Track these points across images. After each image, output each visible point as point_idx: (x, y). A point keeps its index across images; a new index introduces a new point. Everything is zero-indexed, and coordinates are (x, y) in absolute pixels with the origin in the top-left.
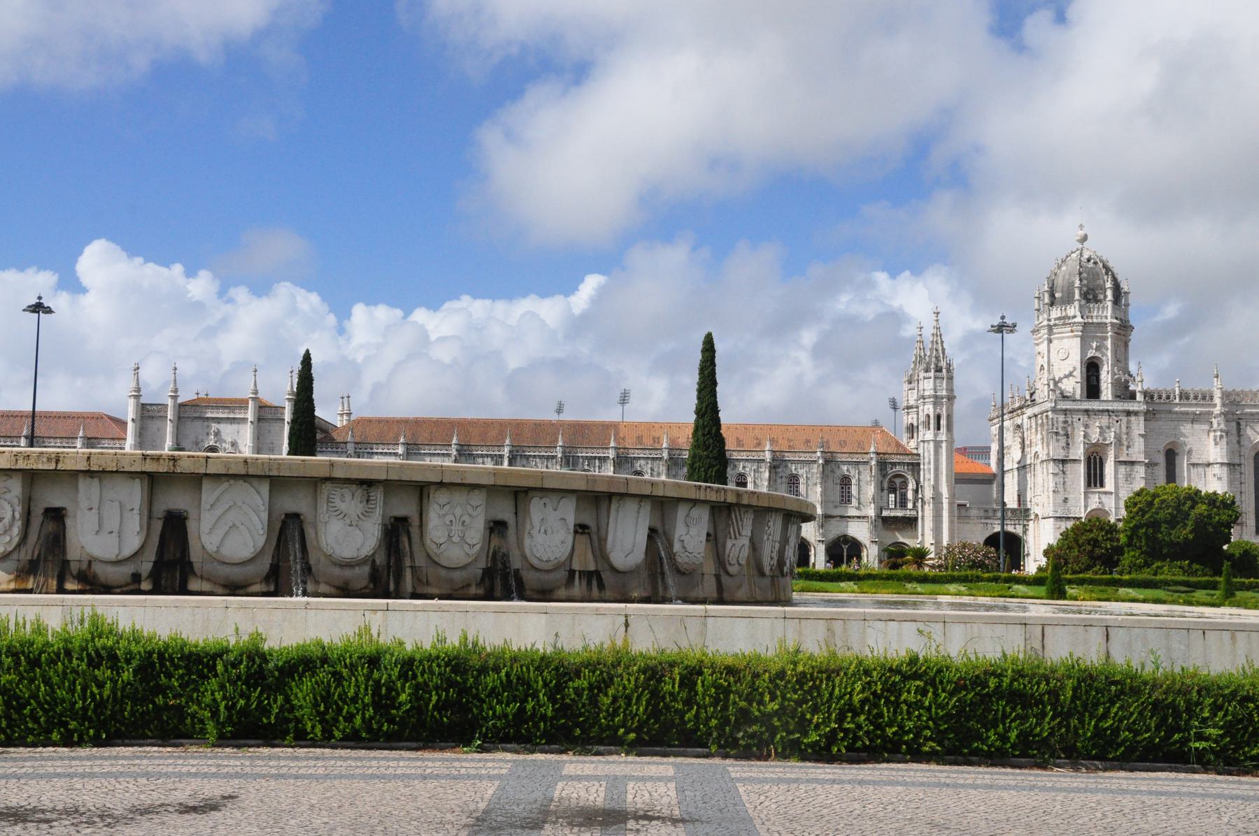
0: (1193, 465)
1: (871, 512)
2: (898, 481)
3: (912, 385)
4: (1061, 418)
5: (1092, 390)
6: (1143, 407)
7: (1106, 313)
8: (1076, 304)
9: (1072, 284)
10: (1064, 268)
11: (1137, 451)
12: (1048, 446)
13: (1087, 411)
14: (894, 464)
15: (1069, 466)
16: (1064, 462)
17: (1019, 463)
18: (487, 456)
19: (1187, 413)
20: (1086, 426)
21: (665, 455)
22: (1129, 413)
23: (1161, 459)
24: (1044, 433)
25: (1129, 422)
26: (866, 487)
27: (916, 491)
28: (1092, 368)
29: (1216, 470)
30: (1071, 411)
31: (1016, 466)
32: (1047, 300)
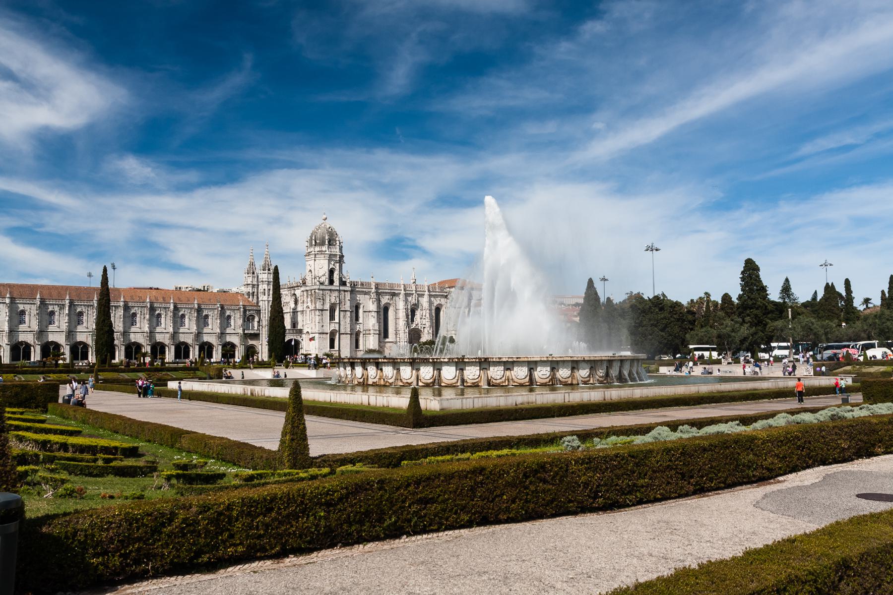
0: (365, 312)
1: (241, 331)
2: (251, 317)
3: (249, 275)
4: (321, 292)
5: (331, 282)
6: (350, 289)
7: (336, 250)
8: (327, 246)
9: (324, 238)
10: (320, 230)
11: (348, 306)
12: (315, 304)
13: (330, 290)
14: (249, 310)
15: (324, 312)
16: (322, 310)
17: (293, 309)
18: (56, 304)
19: (363, 291)
20: (330, 296)
21: (148, 305)
22: (345, 291)
23: (354, 309)
24: (313, 298)
25: (345, 294)
26: (237, 322)
27: (259, 322)
28: (331, 272)
29: (373, 314)
30: (325, 290)
31: (291, 311)
32: (314, 243)
